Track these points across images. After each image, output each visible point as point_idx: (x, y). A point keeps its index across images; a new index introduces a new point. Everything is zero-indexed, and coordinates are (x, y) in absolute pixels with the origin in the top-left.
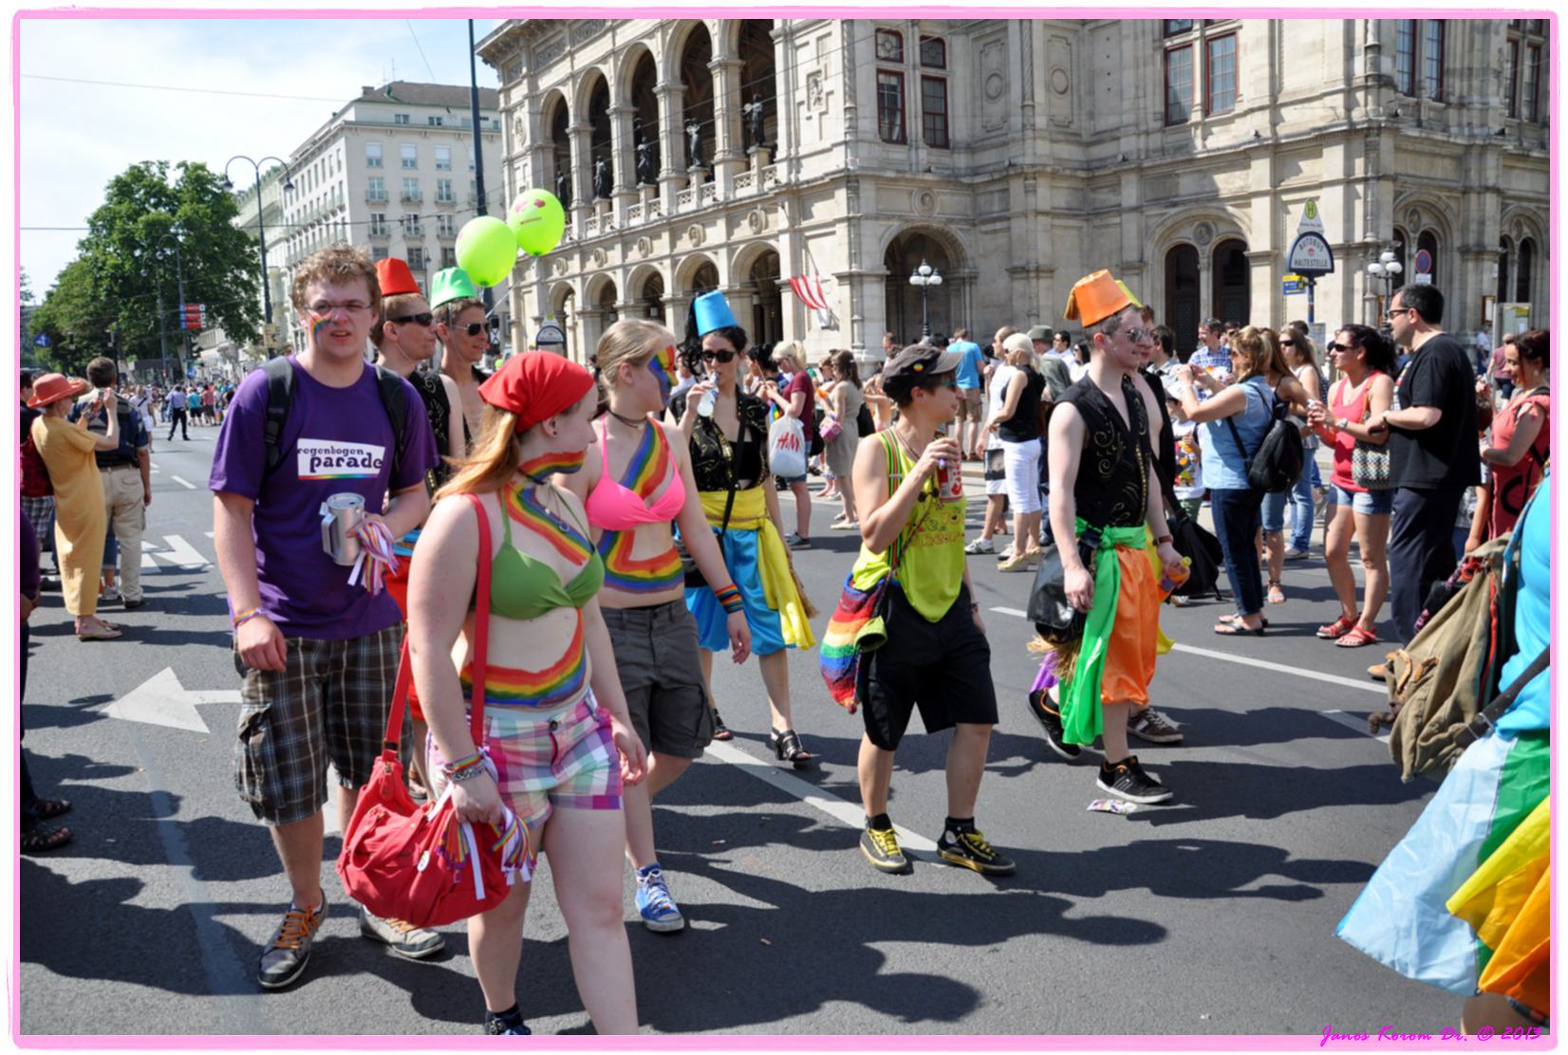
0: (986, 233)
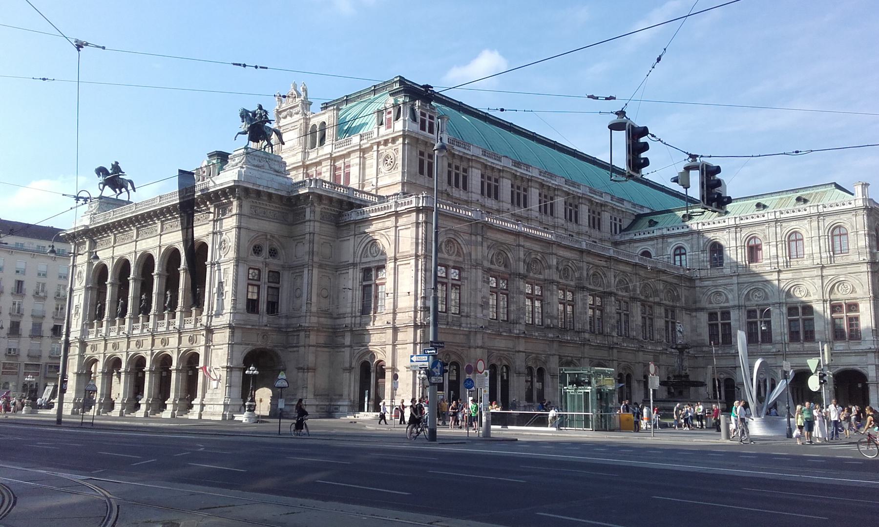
0: (291, 352)
